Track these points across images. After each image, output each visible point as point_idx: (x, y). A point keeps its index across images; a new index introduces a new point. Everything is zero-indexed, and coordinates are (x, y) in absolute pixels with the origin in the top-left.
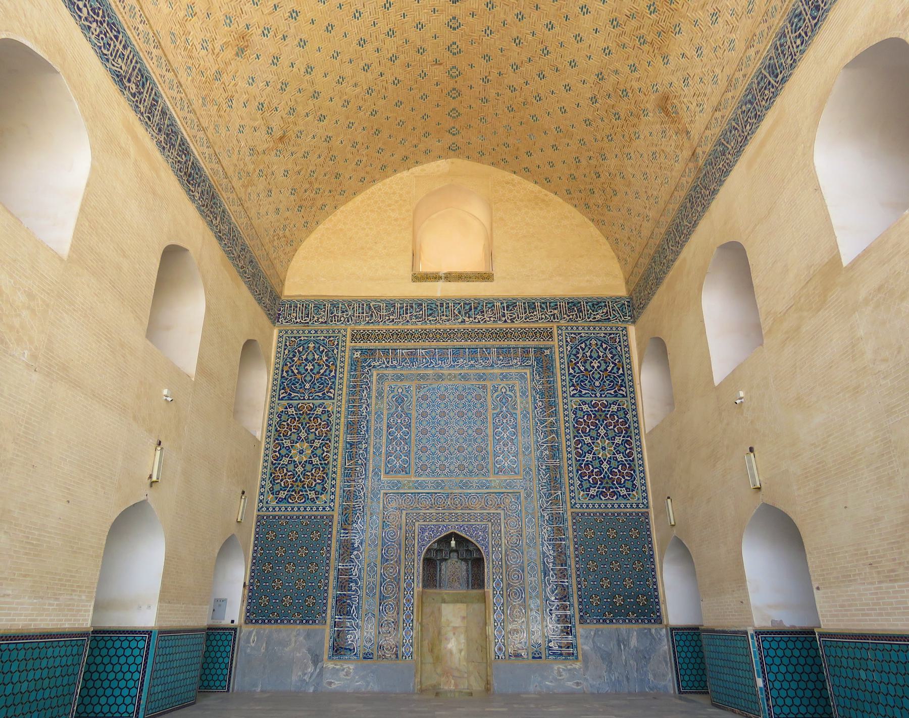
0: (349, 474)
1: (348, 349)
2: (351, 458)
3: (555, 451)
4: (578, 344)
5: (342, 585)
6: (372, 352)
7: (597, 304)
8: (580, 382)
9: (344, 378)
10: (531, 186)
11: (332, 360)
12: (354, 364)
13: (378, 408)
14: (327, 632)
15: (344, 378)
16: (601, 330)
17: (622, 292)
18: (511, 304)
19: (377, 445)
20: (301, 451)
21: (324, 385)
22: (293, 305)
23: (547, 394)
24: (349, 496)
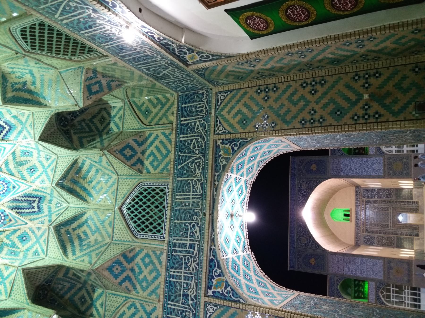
0: (388, 234)
1: (366, 233)
2: (385, 233)
3: (385, 201)
4: (364, 196)
5: (407, 235)
6: (366, 230)
7: (357, 192)
8: (372, 196)
9: (370, 234)
10: (331, 200)
11: (367, 236)
12: (369, 232)
13: (377, 229)
14: (415, 237)
15: (370, 234)
16: (362, 192)
17: (354, 187)
18: (357, 206)
19: (383, 229)
20: (385, 241)
21: (372, 238)
22: (357, 243)
23: (374, 202)
24: (393, 234)
